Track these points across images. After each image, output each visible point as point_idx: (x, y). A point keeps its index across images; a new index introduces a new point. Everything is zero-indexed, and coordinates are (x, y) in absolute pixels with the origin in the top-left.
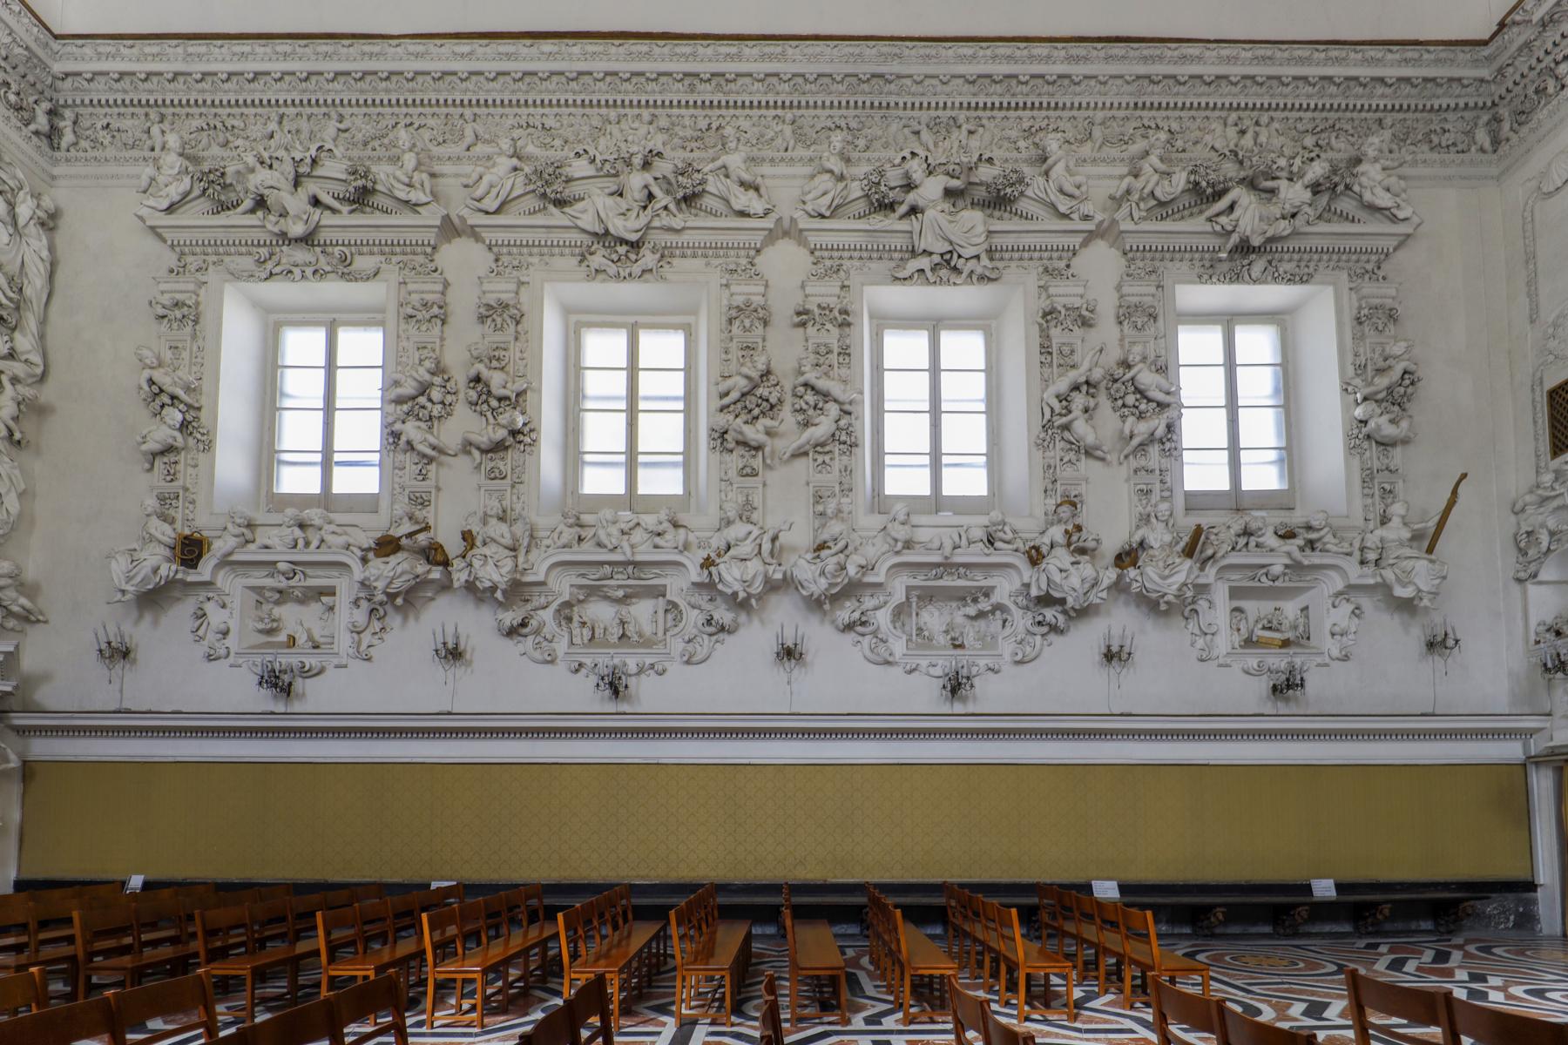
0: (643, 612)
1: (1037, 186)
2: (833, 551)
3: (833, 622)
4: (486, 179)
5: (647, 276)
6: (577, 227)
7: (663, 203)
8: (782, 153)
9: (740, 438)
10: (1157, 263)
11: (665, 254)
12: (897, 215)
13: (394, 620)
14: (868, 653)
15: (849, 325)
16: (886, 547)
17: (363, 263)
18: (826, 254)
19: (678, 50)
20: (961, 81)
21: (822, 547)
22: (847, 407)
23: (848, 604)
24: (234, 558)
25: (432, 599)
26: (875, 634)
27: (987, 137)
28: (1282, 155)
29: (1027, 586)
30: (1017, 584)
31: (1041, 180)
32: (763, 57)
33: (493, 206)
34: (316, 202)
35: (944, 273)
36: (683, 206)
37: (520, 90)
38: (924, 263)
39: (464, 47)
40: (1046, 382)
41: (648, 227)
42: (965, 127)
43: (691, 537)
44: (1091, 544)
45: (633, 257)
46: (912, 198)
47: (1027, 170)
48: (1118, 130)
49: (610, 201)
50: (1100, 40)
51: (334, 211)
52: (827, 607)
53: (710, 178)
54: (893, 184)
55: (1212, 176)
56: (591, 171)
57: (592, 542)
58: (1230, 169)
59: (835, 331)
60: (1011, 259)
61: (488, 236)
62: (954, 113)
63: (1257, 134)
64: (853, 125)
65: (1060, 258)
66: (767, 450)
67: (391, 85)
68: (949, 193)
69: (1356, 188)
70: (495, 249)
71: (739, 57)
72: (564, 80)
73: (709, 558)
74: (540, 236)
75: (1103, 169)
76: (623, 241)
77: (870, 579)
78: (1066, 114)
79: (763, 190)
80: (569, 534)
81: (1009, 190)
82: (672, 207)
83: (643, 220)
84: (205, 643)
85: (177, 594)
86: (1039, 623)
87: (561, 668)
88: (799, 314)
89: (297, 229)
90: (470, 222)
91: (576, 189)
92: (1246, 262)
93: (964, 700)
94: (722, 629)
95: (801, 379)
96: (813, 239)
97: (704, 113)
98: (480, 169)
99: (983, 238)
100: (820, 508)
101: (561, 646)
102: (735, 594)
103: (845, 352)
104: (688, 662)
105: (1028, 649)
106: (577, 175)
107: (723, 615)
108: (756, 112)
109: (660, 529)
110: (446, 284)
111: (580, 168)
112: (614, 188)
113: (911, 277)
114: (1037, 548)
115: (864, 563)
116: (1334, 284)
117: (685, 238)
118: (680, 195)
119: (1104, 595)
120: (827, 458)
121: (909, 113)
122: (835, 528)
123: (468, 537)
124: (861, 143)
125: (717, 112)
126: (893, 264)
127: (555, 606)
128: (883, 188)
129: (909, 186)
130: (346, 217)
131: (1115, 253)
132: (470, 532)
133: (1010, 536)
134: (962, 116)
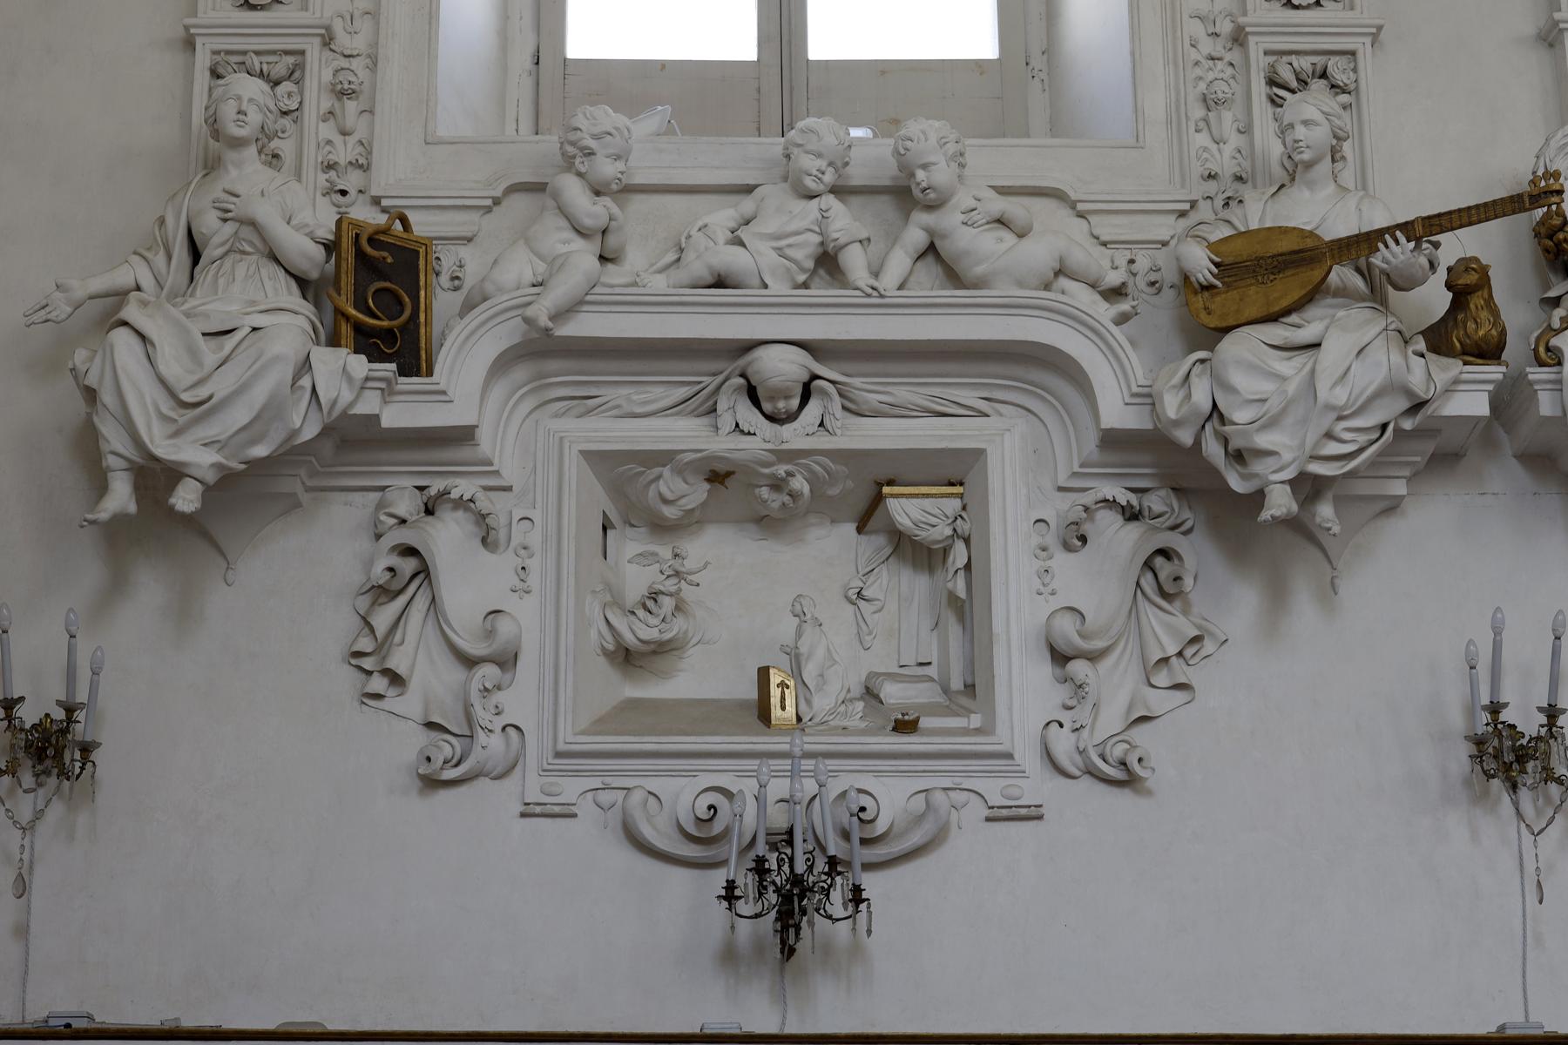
24: (588, 325)
84: (410, 704)
85: (291, 485)
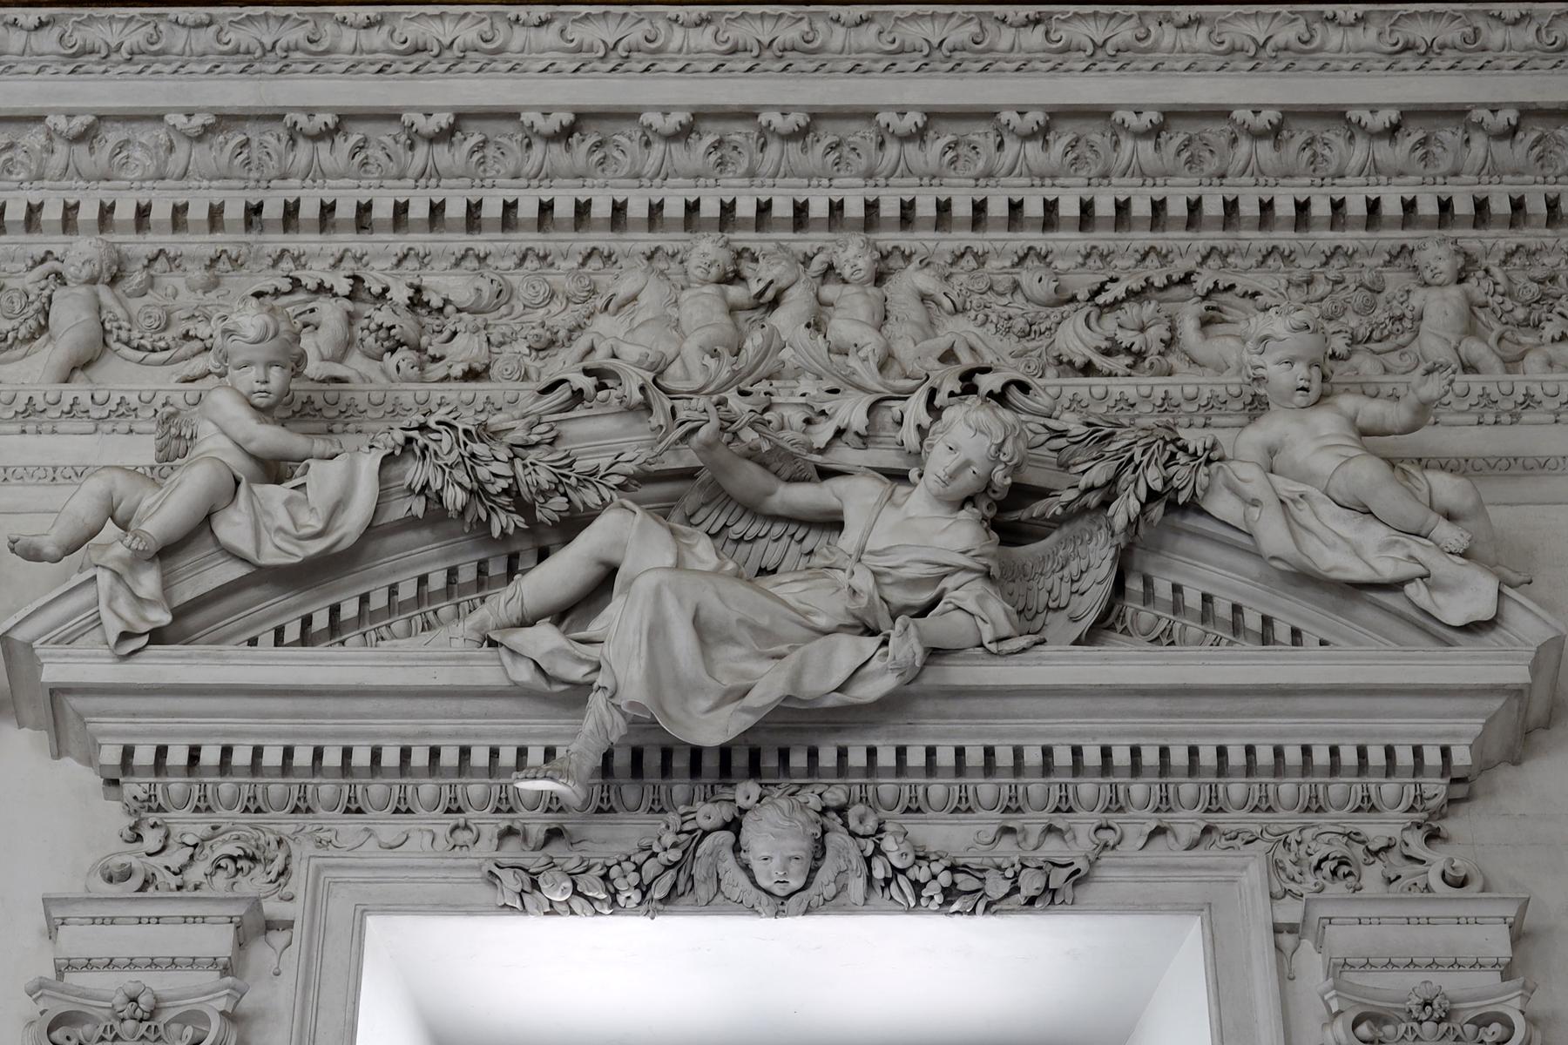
55: (495, 468)
58: (604, 439)
69: (1223, 505)
75: (71, 446)
116: (1205, 908)
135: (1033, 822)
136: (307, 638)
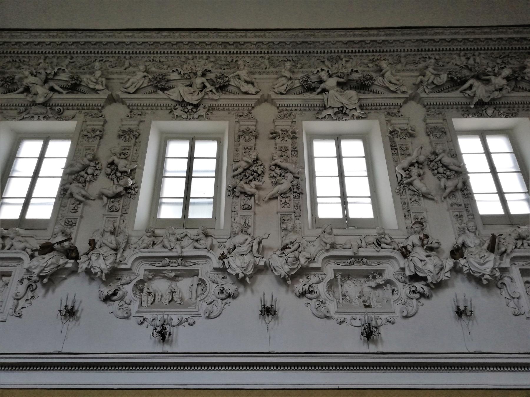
0: (185, 285)
1: (379, 80)
2: (293, 248)
3: (293, 291)
4: (131, 81)
5: (200, 118)
6: (170, 98)
7: (210, 89)
8: (264, 70)
9: (242, 190)
10: (441, 110)
11: (210, 110)
12: (317, 92)
13: (40, 291)
14: (315, 312)
15: (296, 138)
16: (321, 248)
17: (67, 113)
18: (284, 108)
19: (220, 34)
20: (341, 43)
21: (285, 247)
22: (296, 175)
23: (301, 280)
25: (65, 279)
26: (317, 298)
27: (354, 63)
28: (488, 66)
29: (403, 269)
30: (397, 269)
31: (381, 78)
32: (256, 36)
33: (132, 90)
34: (52, 89)
35: (340, 115)
36: (220, 91)
37: (152, 48)
38: (330, 112)
39: (130, 34)
40: (396, 162)
41: (203, 98)
42: (344, 59)
43: (215, 242)
44: (435, 245)
45: (194, 110)
46: (322, 86)
47: (374, 75)
48: (412, 59)
49: (186, 88)
50: (398, 28)
51: (60, 93)
52: (289, 282)
53: (232, 79)
54: (313, 81)
55: (459, 75)
56: (178, 77)
57: (160, 245)
58: (466, 72)
59: (289, 141)
60: (371, 109)
61: (128, 102)
62: (339, 55)
63: (475, 60)
64: (294, 59)
65: (394, 109)
66: (256, 196)
67: (97, 46)
68: (339, 84)
70: (131, 108)
71: (246, 36)
72: (171, 44)
73: (224, 253)
74: (153, 102)
76: (190, 104)
77: (313, 265)
78: (388, 54)
79: (255, 84)
80: (148, 241)
81: (367, 82)
82: (214, 91)
83: (201, 96)
86: (414, 292)
87: (133, 321)
88: (272, 133)
89: (41, 100)
90: (121, 97)
91: (172, 84)
92: (483, 109)
93: (375, 342)
94: (229, 296)
95: (273, 163)
96: (278, 103)
97: (230, 56)
98: (129, 77)
99: (357, 101)
100: (284, 226)
101: (134, 308)
102: (237, 275)
103: (295, 150)
104: (208, 317)
105: (410, 308)
106: (172, 79)
107: (230, 287)
108: (252, 55)
109: (198, 238)
110: (105, 122)
111: (174, 76)
112: (188, 83)
113: (325, 117)
114: (405, 247)
115: (309, 256)
117: (220, 102)
118: (218, 86)
119: (448, 274)
120: (287, 200)
121: (319, 55)
122: (292, 237)
123: (92, 243)
124: (299, 66)
125: (236, 55)
126: (316, 112)
127: (134, 282)
128: (309, 82)
129: (321, 81)
130: (65, 95)
131: (419, 106)
132: (94, 240)
133: (389, 241)
134: (342, 56)
135: (511, 109)
136: (439, 92)
